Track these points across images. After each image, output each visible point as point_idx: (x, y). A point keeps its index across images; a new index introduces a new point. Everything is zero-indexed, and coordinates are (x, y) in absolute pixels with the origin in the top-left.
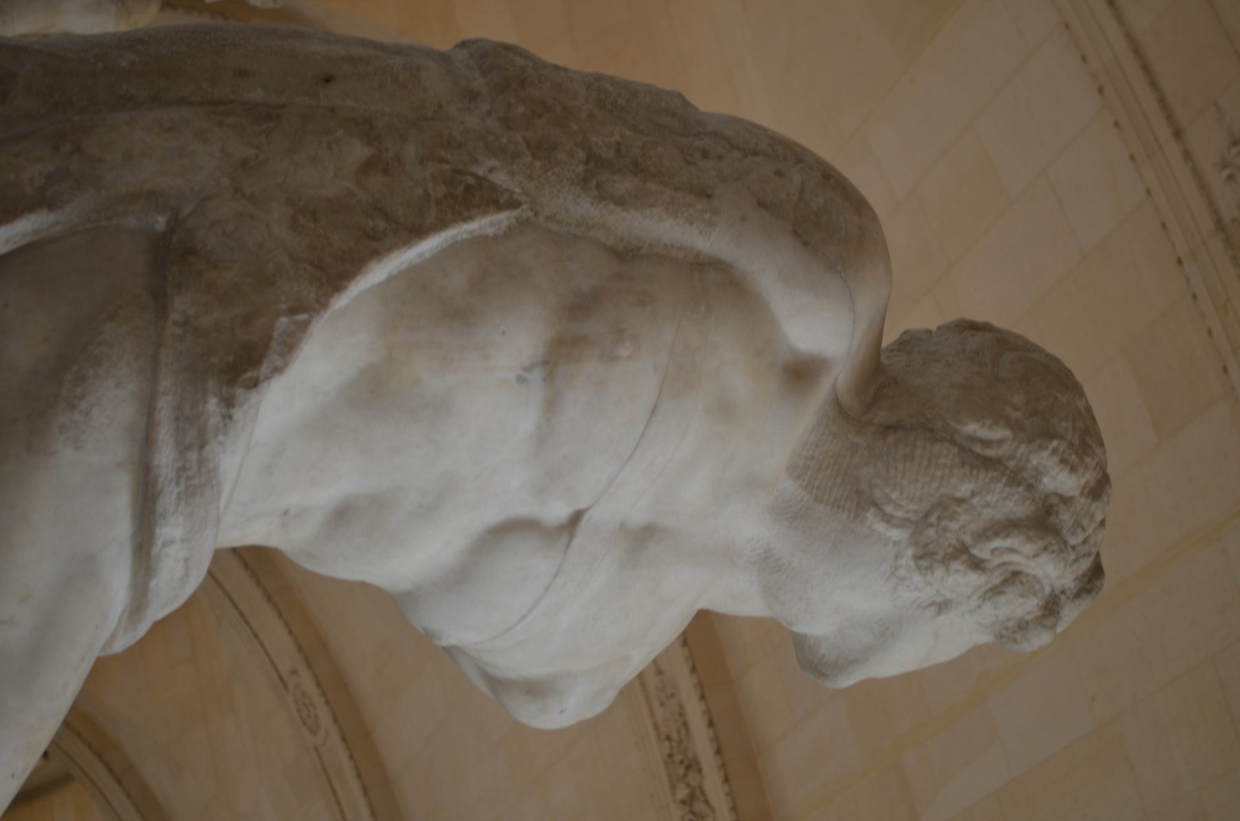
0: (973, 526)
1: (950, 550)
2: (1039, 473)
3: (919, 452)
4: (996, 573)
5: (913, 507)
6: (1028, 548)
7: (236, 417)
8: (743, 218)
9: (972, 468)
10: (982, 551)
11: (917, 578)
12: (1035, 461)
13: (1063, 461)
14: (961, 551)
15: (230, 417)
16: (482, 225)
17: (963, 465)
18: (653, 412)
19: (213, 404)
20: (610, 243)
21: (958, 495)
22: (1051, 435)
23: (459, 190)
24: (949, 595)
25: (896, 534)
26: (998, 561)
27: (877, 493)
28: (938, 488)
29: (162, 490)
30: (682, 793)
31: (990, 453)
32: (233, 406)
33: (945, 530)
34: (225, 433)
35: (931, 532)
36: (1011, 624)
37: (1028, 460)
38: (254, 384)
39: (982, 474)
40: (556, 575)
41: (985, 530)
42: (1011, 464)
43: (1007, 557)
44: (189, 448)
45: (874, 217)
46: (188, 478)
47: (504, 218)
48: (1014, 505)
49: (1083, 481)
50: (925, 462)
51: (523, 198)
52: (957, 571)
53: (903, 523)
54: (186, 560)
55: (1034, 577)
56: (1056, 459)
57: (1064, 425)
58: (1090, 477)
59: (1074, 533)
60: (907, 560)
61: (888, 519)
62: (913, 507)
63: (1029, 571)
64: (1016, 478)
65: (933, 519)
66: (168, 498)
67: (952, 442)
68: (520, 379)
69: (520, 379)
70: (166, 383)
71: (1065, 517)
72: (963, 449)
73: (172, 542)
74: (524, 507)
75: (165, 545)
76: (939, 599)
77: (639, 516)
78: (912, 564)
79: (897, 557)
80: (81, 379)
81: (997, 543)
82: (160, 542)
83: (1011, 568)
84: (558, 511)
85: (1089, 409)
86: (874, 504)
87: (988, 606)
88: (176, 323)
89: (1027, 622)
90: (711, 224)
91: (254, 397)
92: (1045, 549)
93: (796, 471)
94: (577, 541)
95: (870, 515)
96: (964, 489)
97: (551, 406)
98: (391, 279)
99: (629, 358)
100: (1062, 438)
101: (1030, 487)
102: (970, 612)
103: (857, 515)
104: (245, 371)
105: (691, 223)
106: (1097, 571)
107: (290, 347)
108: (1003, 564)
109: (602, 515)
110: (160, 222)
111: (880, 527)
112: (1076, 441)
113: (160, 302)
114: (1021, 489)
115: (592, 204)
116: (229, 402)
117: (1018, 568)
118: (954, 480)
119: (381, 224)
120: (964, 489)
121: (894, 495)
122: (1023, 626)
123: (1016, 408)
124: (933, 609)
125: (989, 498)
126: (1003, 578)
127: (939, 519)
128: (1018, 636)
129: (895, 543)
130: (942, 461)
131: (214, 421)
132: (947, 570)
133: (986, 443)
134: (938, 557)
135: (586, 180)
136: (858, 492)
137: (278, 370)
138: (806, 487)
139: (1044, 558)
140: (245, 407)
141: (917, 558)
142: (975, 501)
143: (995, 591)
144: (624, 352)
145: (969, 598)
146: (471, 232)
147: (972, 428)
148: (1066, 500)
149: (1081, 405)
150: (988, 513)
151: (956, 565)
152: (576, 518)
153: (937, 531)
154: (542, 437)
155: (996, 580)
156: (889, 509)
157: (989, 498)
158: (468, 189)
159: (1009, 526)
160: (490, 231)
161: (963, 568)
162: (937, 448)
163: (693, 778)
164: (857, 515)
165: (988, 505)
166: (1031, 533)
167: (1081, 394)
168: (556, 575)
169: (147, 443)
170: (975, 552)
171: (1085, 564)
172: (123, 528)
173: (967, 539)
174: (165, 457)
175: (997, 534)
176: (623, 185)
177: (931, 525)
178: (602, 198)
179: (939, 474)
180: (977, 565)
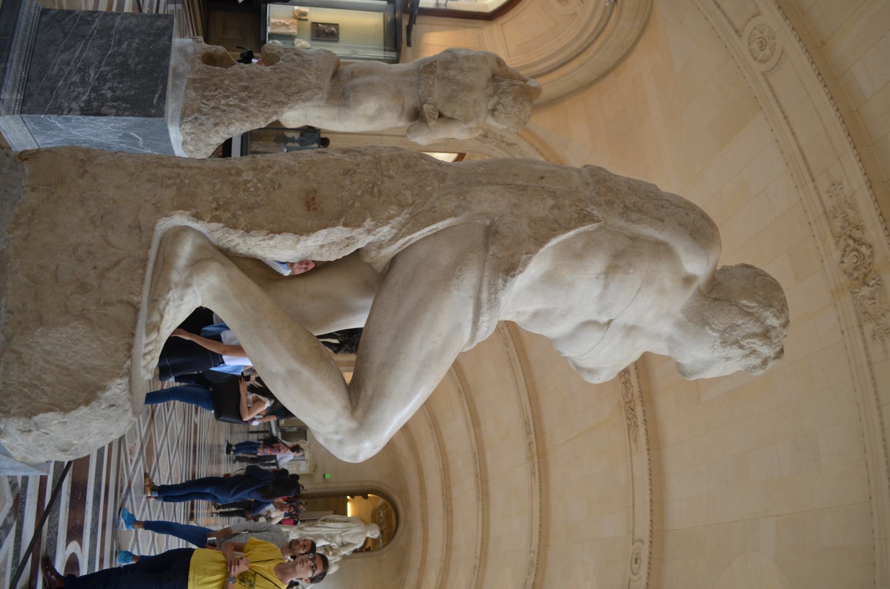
0: (741, 334)
1: (733, 342)
2: (766, 318)
3: (725, 309)
4: (748, 350)
5: (722, 326)
6: (760, 343)
8: (674, 229)
9: (743, 315)
10: (744, 343)
11: (721, 349)
12: (765, 314)
13: (775, 315)
14: (737, 342)
15: (505, 286)
16: (588, 227)
17: (740, 314)
18: (639, 291)
19: (500, 281)
20: (629, 235)
21: (737, 323)
22: (771, 306)
23: (582, 216)
24: (731, 356)
25: (715, 334)
26: (749, 346)
27: (710, 320)
28: (731, 321)
29: (483, 306)
30: (623, 380)
31: (750, 310)
34: (503, 290)
35: (727, 335)
36: (750, 366)
37: (762, 314)
38: (514, 276)
39: (746, 318)
40: (602, 339)
41: (746, 336)
42: (757, 315)
43: (754, 346)
44: (492, 294)
45: (717, 230)
46: (491, 303)
47: (595, 225)
48: (756, 328)
49: (781, 322)
52: (735, 348)
53: (718, 331)
55: (760, 352)
56: (772, 314)
57: (776, 303)
58: (783, 321)
59: (775, 339)
60: (718, 343)
61: (713, 329)
62: (722, 326)
63: (759, 350)
64: (758, 320)
65: (728, 331)
67: (737, 306)
68: (597, 278)
69: (597, 278)
70: (486, 273)
71: (773, 333)
73: (484, 322)
74: (594, 317)
75: (482, 322)
76: (727, 356)
77: (630, 322)
78: (719, 344)
79: (715, 342)
81: (749, 340)
82: (481, 322)
83: (753, 349)
84: (604, 319)
85: (784, 297)
86: (709, 324)
87: (744, 360)
88: (491, 255)
89: (756, 366)
90: (663, 230)
91: (513, 280)
92: (765, 344)
93: (683, 311)
95: (707, 328)
96: (740, 322)
97: (606, 287)
98: (558, 243)
99: (632, 273)
100: (775, 308)
101: (762, 323)
102: (737, 361)
103: (702, 328)
104: (511, 272)
105: (656, 230)
106: (782, 351)
107: (525, 265)
108: (750, 347)
109: (619, 321)
110: (488, 222)
111: (710, 332)
112: (779, 309)
113: (487, 250)
114: (759, 323)
116: (505, 281)
117: (755, 349)
118: (736, 319)
119: (556, 226)
120: (740, 322)
121: (715, 322)
122: (755, 367)
123: (759, 296)
124: (725, 359)
125: (748, 326)
127: (730, 331)
128: (753, 370)
129: (714, 337)
130: (733, 312)
131: (500, 286)
132: (731, 348)
133: (749, 307)
135: (623, 214)
136: (704, 320)
137: (521, 272)
138: (686, 317)
139: (765, 347)
140: (510, 283)
141: (721, 343)
142: (743, 326)
143: (747, 356)
144: (631, 271)
145: (737, 357)
147: (744, 302)
148: (774, 328)
149: (782, 296)
150: (747, 330)
151: (734, 346)
152: (610, 322)
154: (602, 297)
155: (747, 352)
156: (713, 326)
157: (748, 326)
158: (585, 215)
159: (754, 335)
160: (591, 229)
163: (627, 376)
164: (702, 328)
165: (747, 328)
166: (761, 338)
167: (783, 292)
168: (602, 339)
169: (479, 291)
170: (741, 343)
171: (778, 349)
172: (470, 316)
173: (739, 338)
174: (484, 296)
175: (749, 338)
176: (635, 216)
177: (727, 333)
178: (628, 220)
179: (732, 316)
180: (741, 347)
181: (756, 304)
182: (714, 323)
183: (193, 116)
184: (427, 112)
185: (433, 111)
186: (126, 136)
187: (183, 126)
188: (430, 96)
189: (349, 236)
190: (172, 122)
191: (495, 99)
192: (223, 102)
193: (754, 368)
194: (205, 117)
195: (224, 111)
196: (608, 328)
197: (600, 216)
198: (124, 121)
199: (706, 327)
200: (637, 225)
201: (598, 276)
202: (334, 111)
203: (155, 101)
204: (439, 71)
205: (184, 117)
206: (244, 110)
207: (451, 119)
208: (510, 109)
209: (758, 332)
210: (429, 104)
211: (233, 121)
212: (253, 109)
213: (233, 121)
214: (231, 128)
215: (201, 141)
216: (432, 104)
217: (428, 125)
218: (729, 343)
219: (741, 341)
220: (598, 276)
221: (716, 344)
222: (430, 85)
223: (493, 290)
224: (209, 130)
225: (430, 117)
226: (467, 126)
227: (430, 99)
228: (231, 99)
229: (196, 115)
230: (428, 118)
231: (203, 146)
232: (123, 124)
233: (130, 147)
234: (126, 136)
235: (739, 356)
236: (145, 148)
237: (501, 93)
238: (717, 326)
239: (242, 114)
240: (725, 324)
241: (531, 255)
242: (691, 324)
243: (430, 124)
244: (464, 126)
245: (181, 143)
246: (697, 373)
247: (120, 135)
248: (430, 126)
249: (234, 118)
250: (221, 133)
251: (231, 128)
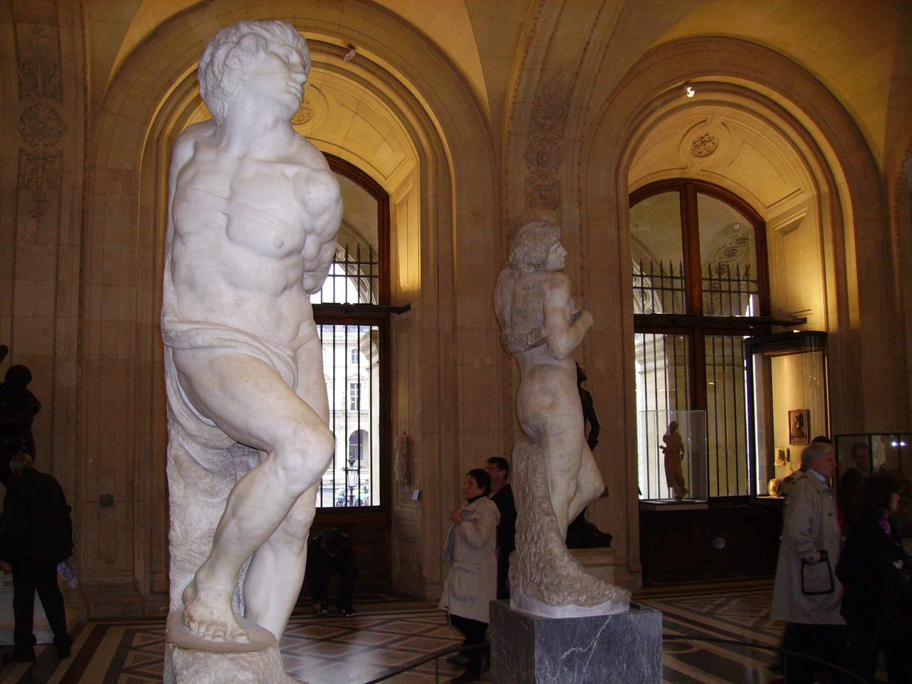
68: (184, 245)
97: (189, 234)
146: (169, 263)
183: (543, 591)
186: (569, 662)
187: (553, 602)
189: (173, 462)
190: (551, 614)
191: (521, 266)
192: (532, 560)
194: (544, 578)
195: (539, 558)
198: (540, 661)
202: (552, 440)
203: (527, 628)
205: (544, 601)
206: (539, 538)
208: (526, 248)
211: (547, 550)
212: (539, 527)
213: (547, 550)
214: (556, 553)
215: (572, 586)
217: (547, 337)
224: (558, 575)
226: (548, 291)
227: (524, 338)
228: (531, 550)
229: (543, 588)
231: (579, 584)
232: (546, 663)
233: (588, 663)
234: (569, 662)
236: (589, 646)
239: (540, 539)
245: (579, 607)
247: (566, 670)
249: (545, 548)
250: (562, 564)
251: (556, 553)
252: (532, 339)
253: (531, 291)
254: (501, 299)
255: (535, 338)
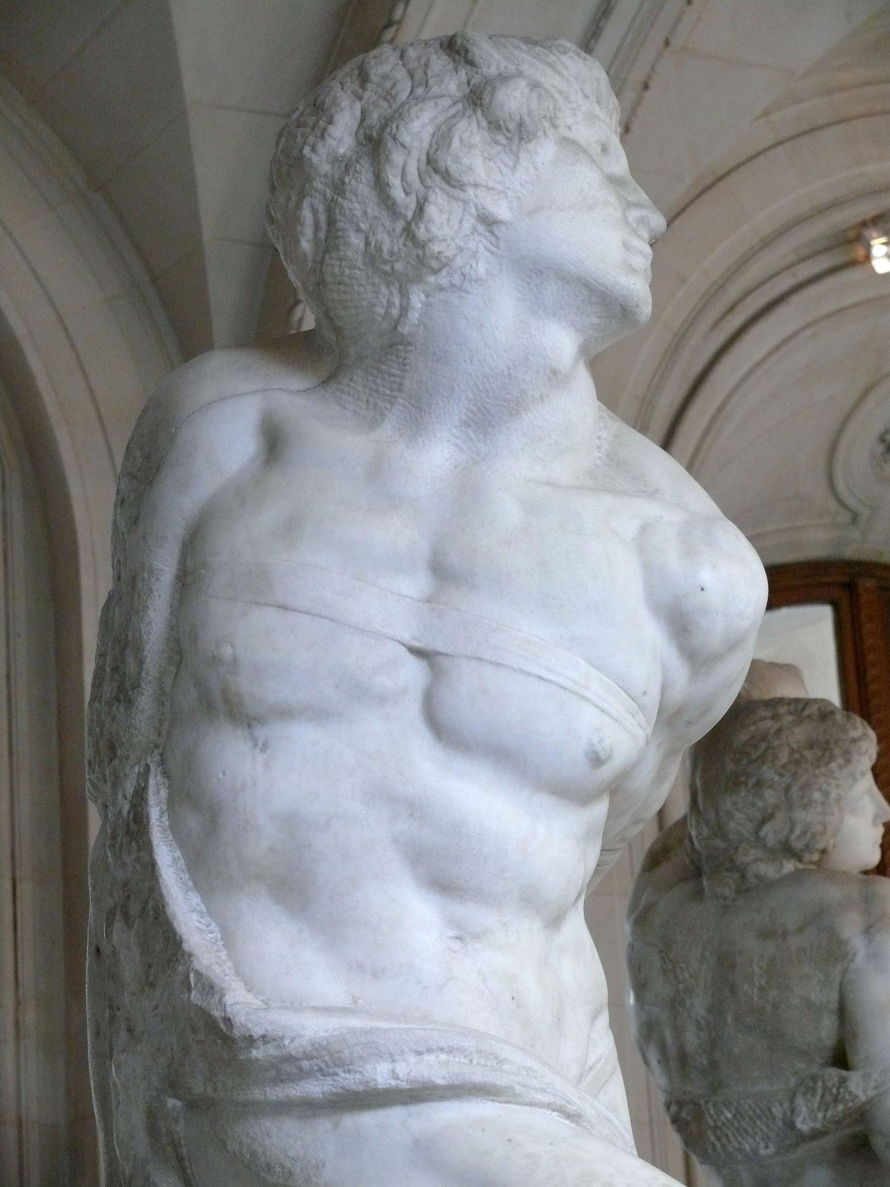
0: (387, 224)
1: (410, 244)
2: (335, 159)
3: (336, 296)
4: (429, 182)
5: (384, 290)
6: (398, 157)
7: (261, 1032)
12: (326, 168)
15: (263, 1036)
17: (337, 248)
21: (362, 246)
25: (417, 299)
26: (417, 185)
28: (359, 269)
29: (343, 1088)
32: (251, 1036)
33: (392, 253)
35: (399, 266)
37: (326, 176)
41: (388, 208)
42: (329, 193)
44: (300, 1069)
50: (342, 287)
51: (142, 762)
52: (428, 230)
53: (404, 294)
54: (420, 1053)
60: (443, 279)
61: (404, 310)
63: (426, 145)
65: (387, 268)
66: (349, 1081)
67: (322, 263)
68: (264, 748)
69: (264, 748)
72: (326, 251)
73: (393, 1071)
74: (413, 709)
75: (397, 1077)
76: (481, 228)
78: (444, 272)
79: (441, 289)
80: (269, 1167)
82: (394, 1083)
89: (490, 123)
90: (151, 571)
92: (394, 138)
94: (440, 647)
95: (404, 329)
97: (285, 713)
99: (233, 646)
103: (409, 344)
111: (414, 316)
114: (347, 180)
115: (143, 694)
116: (250, 1041)
117: (424, 158)
118: (349, 254)
120: (356, 241)
121: (381, 311)
123: (289, 199)
124: (496, 230)
125: (358, 213)
126: (433, 174)
127: (385, 262)
128: (512, 126)
129: (427, 295)
131: (272, 1050)
134: (420, 252)
138: (392, 404)
140: (250, 1026)
146: (162, 813)
147: (306, 245)
152: (418, 652)
153: (396, 261)
156: (395, 312)
159: (380, 185)
160: (164, 793)
161: (422, 226)
162: (329, 278)
164: (409, 344)
166: (383, 158)
170: (410, 214)
172: (394, 1115)
173: (400, 225)
174: (315, 1088)
177: (393, 268)
179: (347, 271)
181: (305, 205)
182: (387, 313)
184: (820, 1115)
185: (814, 1090)
188: (770, 1110)
191: (748, 856)
193: (499, 128)
196: (442, 654)
197: (137, 770)
199: (405, 332)
200: (146, 653)
201: (260, 744)
204: (696, 1088)
207: (843, 1013)
209: (370, 175)
210: (793, 1111)
216: (792, 1101)
218: (420, 252)
219: (406, 216)
220: (260, 744)
221: (444, 281)
222: (734, 1116)
223: (287, 1068)
225: (836, 1100)
227: (777, 1111)
230: (840, 1107)
235: (457, 199)
237: (725, 837)
238: (389, 301)
240: (374, 284)
241: (192, 976)
242: (407, 383)
243: (863, 1098)
244: (860, 959)
246: (588, 286)
248: (871, 1093)
252: (812, 1111)
253: (793, 942)
254: (665, 971)
255: (824, 1106)
